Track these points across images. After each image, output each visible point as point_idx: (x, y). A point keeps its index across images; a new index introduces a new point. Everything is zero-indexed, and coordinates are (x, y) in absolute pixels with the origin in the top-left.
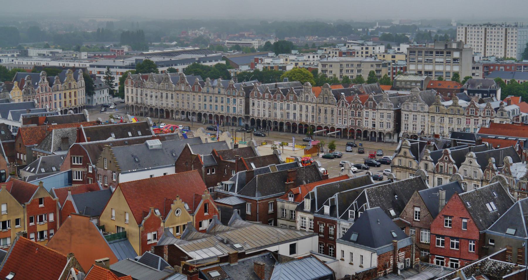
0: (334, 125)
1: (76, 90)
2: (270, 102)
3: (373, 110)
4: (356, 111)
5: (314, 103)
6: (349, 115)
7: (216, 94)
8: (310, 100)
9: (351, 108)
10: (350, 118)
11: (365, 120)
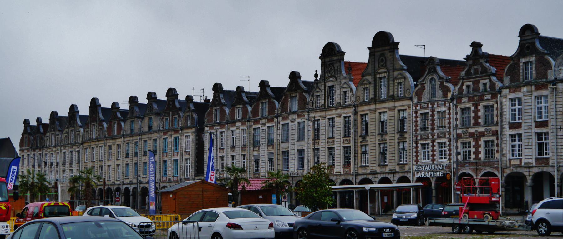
0: (407, 168)
2: (245, 127)
3: (537, 88)
4: (476, 105)
5: (349, 106)
6: (453, 123)
8: (338, 100)
9: (457, 99)
10: (459, 136)
11: (508, 132)
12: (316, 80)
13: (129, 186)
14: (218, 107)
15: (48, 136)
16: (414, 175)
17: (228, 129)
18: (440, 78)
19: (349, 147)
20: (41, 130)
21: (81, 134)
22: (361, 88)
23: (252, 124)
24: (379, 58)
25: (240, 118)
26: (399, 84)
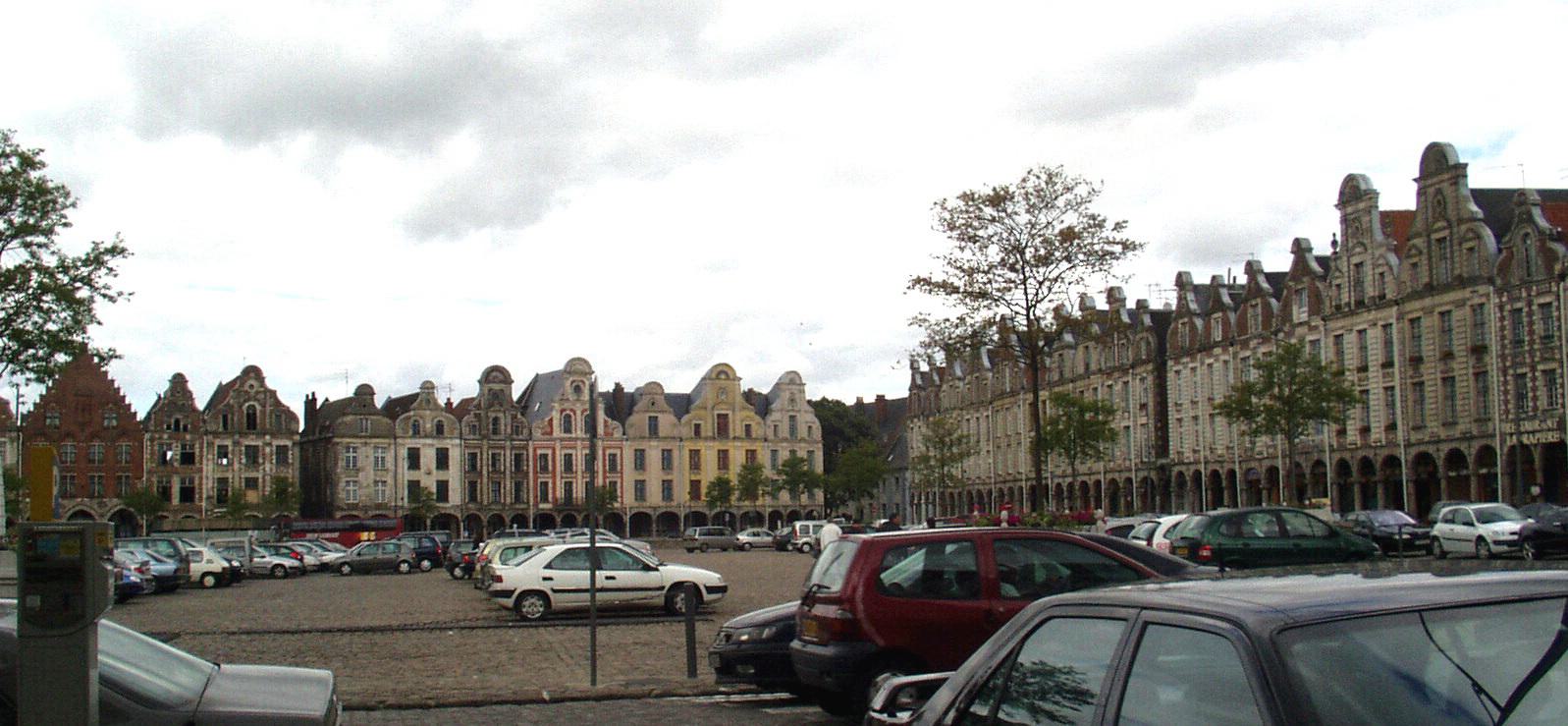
1: (757, 446)
7: (1081, 377)
12: (1335, 253)
13: (1060, 480)
14: (1186, 320)
15: (944, 391)
16: (1503, 442)
17: (1202, 363)
18: (1541, 232)
19: (1393, 388)
20: (936, 378)
21: (989, 382)
22: (1407, 263)
23: (1238, 349)
24: (1434, 198)
25: (1220, 339)
26: (1471, 249)
